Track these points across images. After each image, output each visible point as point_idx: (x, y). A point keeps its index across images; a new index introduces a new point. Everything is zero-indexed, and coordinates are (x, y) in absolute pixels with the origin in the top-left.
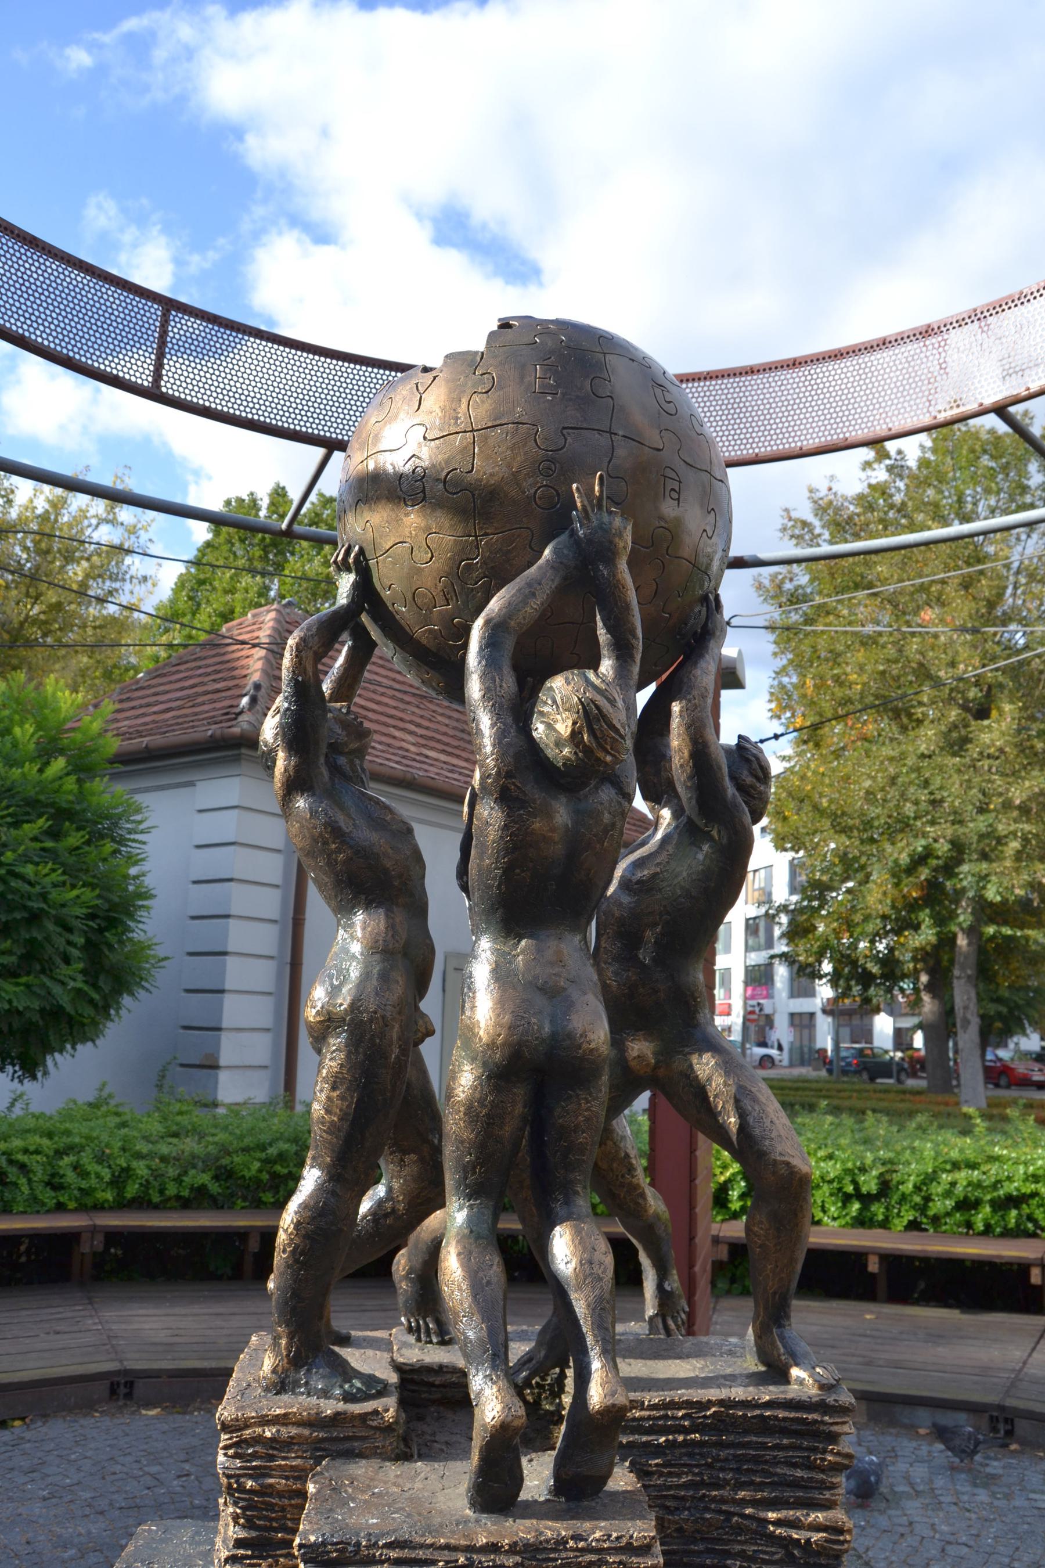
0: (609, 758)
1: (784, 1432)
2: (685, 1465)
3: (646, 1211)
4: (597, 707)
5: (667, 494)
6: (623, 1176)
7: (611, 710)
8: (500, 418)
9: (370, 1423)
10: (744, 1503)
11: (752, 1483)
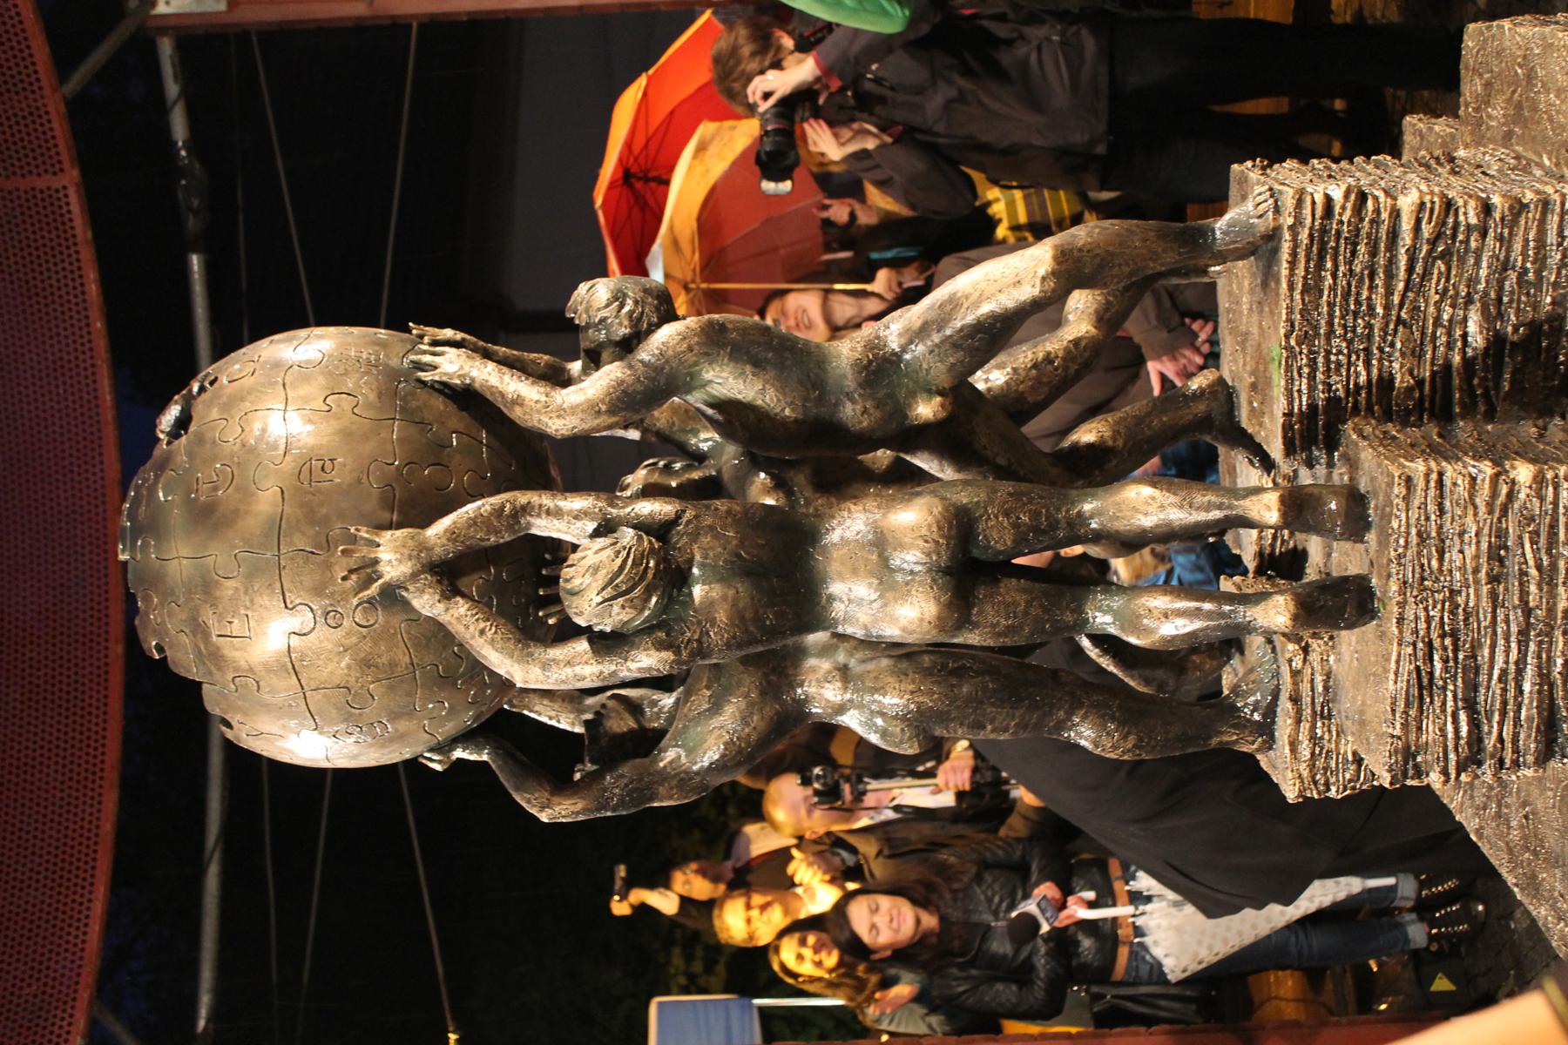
0: (652, 564)
1: (1320, 266)
2: (1348, 370)
4: (603, 589)
5: (329, 477)
6: (1056, 369)
7: (604, 571)
8: (287, 670)
9: (1299, 667)
10: (1387, 307)
11: (1369, 299)
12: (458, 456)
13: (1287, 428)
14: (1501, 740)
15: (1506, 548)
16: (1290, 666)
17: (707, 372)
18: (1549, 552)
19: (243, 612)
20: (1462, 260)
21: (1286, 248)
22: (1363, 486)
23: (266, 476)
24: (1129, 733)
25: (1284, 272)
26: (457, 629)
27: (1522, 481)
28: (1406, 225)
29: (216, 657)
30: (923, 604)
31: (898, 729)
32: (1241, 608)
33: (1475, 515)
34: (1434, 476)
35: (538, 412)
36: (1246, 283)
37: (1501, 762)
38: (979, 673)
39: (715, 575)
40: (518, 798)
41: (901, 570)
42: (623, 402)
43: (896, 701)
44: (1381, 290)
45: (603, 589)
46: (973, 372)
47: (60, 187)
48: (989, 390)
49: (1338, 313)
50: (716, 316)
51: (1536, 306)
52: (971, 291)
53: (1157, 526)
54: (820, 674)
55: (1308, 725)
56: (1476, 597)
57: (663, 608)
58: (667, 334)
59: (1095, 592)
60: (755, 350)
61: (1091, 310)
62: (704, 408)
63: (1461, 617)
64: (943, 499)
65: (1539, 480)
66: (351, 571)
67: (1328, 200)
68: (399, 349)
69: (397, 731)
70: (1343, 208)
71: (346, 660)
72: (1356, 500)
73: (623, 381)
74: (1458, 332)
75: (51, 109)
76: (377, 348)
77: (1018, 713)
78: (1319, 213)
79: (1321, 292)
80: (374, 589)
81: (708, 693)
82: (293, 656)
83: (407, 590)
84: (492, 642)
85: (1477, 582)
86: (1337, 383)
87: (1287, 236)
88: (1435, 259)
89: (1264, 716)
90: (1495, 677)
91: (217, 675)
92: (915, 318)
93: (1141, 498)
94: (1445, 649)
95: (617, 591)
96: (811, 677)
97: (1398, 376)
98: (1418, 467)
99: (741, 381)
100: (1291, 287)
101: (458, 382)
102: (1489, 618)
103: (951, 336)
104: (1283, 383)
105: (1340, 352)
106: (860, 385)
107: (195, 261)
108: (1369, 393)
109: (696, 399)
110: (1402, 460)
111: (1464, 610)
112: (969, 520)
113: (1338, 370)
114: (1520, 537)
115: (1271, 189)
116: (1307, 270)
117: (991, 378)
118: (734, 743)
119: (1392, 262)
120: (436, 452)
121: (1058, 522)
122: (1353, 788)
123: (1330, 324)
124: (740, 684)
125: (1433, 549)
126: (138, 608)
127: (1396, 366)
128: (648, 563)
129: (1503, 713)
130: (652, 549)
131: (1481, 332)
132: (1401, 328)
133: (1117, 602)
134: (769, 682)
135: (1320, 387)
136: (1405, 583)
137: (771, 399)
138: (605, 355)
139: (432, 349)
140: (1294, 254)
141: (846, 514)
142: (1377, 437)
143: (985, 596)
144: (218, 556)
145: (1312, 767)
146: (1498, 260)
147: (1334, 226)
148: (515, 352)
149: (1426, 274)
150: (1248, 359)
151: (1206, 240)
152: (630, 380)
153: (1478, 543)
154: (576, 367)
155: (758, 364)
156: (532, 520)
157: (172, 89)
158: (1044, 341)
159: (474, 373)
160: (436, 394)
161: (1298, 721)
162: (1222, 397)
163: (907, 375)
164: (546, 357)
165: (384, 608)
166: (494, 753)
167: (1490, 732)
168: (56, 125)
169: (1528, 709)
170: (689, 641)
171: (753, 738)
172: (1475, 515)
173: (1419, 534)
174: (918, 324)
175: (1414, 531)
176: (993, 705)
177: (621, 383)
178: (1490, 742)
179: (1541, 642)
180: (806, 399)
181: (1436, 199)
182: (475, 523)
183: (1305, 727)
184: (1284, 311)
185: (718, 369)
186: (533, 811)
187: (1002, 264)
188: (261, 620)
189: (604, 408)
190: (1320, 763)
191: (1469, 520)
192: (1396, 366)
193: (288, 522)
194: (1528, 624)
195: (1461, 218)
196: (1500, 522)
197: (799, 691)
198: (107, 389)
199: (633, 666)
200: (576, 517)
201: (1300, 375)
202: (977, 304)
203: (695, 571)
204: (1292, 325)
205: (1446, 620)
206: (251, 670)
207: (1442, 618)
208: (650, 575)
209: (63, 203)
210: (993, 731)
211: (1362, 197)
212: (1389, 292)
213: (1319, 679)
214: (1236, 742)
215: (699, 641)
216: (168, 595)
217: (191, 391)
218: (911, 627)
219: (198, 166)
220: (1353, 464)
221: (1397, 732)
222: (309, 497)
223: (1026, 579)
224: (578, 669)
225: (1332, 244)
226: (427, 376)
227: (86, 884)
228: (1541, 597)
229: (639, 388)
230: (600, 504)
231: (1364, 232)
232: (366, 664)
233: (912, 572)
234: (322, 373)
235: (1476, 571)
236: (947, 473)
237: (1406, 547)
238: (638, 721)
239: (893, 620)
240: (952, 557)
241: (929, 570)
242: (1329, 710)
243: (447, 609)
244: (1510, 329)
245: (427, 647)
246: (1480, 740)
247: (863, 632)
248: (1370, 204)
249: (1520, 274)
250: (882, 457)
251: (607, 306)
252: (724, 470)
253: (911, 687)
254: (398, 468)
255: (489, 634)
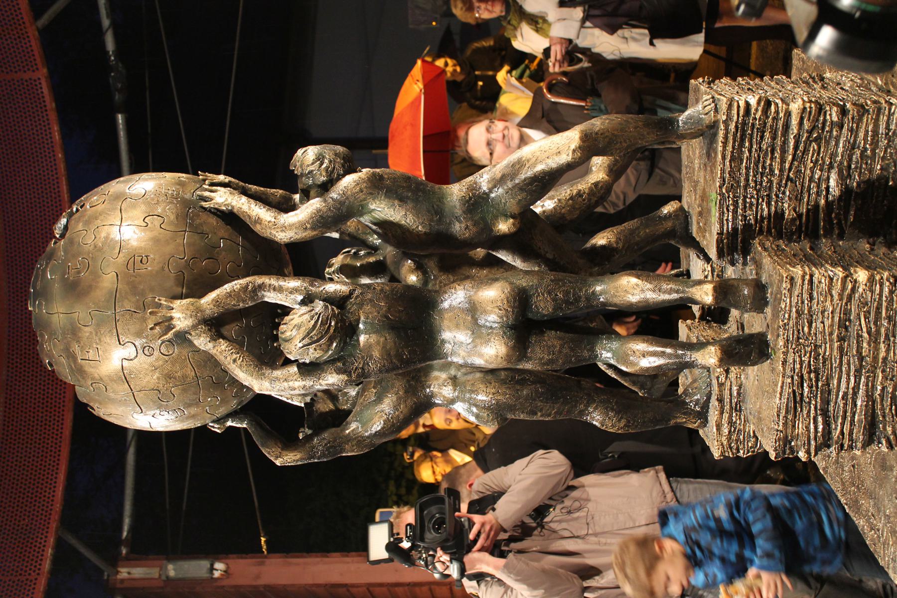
0: (333, 324)
1: (742, 145)
2: (757, 208)
3: (606, 181)
4: (303, 339)
6: (584, 200)
10: (781, 170)
11: (771, 165)
12: (224, 253)
13: (719, 242)
14: (842, 433)
15: (850, 321)
16: (718, 381)
17: (372, 204)
18: (875, 324)
19: (95, 346)
20: (828, 143)
21: (721, 134)
22: (764, 279)
23: (108, 266)
24: (622, 418)
25: (720, 149)
26: (221, 358)
27: (861, 281)
28: (794, 121)
29: (80, 371)
30: (497, 347)
31: (486, 415)
32: (689, 353)
33: (832, 301)
34: (807, 277)
35: (270, 228)
36: (697, 152)
37: (842, 446)
38: (533, 383)
39: (372, 329)
40: (264, 451)
41: (484, 326)
42: (320, 223)
43: (484, 398)
44: (778, 160)
45: (303, 339)
46: (533, 203)
47: (36, 78)
48: (544, 212)
49: (751, 174)
50: (378, 170)
51: (871, 171)
52: (531, 157)
53: (639, 302)
54: (441, 381)
55: (727, 415)
56: (830, 350)
57: (342, 348)
58: (349, 180)
59: (602, 339)
60: (400, 191)
61: (606, 165)
62: (370, 225)
63: (821, 361)
64: (511, 283)
65: (871, 280)
66: (156, 325)
67: (748, 104)
68: (192, 187)
69: (190, 413)
70: (757, 110)
71: (157, 375)
72: (759, 288)
73: (320, 210)
74: (824, 186)
75: (30, 34)
76: (178, 187)
77: (557, 406)
78: (741, 113)
79: (742, 160)
80: (170, 335)
81: (375, 391)
82: (125, 372)
83: (191, 334)
84: (240, 366)
85: (831, 340)
86: (749, 215)
87: (722, 127)
88: (811, 142)
89: (702, 408)
90: (840, 396)
91: (82, 382)
92: (497, 172)
93: (630, 285)
94: (811, 380)
95: (311, 339)
96: (435, 382)
97: (787, 212)
98: (798, 271)
99: (392, 210)
100: (724, 158)
101: (224, 208)
102: (838, 361)
103: (518, 184)
104: (717, 214)
105: (752, 197)
106: (464, 212)
107: (120, 118)
108: (769, 221)
109: (366, 219)
110: (788, 266)
111: (823, 357)
112: (527, 296)
113: (751, 208)
114: (859, 315)
115: (713, 97)
116: (733, 148)
117: (545, 205)
118: (389, 421)
119: (785, 143)
120: (211, 251)
121: (580, 297)
122: (753, 452)
123: (747, 180)
124: (393, 386)
125: (806, 320)
126: (38, 341)
127: (786, 205)
128: (331, 323)
129: (844, 418)
130: (334, 315)
131: (838, 186)
132: (789, 183)
133: (615, 345)
134: (410, 385)
135: (740, 218)
136: (788, 340)
137: (411, 220)
138: (312, 193)
139: (210, 188)
140: (726, 137)
141: (453, 291)
142: (772, 248)
143: (536, 341)
144: (81, 313)
145: (729, 439)
146: (849, 143)
147: (751, 121)
148: (262, 189)
149: (806, 151)
150: (697, 197)
151: (673, 128)
152: (325, 209)
153: (833, 317)
154: (297, 197)
155: (402, 200)
156: (265, 293)
157: (106, 22)
158: (578, 182)
159: (234, 203)
160: (211, 216)
161: (722, 413)
162: (682, 218)
163: (493, 206)
164: (281, 191)
165: (178, 344)
166: (253, 421)
167: (836, 429)
168: (33, 43)
169: (859, 416)
170: (356, 368)
171: (401, 417)
172: (832, 301)
173: (797, 312)
174: (499, 175)
175: (794, 310)
176: (541, 401)
177: (319, 211)
178: (836, 434)
179: (868, 377)
180: (431, 220)
181: (813, 105)
182: (230, 296)
183: (726, 416)
184: (719, 172)
185: (378, 203)
186: (272, 459)
187: (549, 141)
188: (105, 351)
189: (309, 226)
190: (734, 437)
191: (828, 303)
192: (786, 205)
193: (120, 293)
194: (861, 366)
195: (828, 117)
196: (847, 305)
197: (428, 390)
198: (65, 191)
199: (323, 383)
200: (291, 293)
201: (728, 210)
202: (534, 165)
203: (361, 326)
204: (724, 180)
205: (812, 363)
206: (101, 379)
207: (809, 362)
208: (332, 330)
209: (38, 88)
210: (541, 416)
211: (768, 103)
212: (783, 161)
213: (735, 388)
214: (685, 422)
215: (363, 368)
216: (52, 334)
217: (72, 210)
218: (492, 360)
219: (120, 65)
220: (758, 265)
221: (781, 428)
222: (133, 278)
223: (560, 331)
224: (291, 384)
225: (749, 132)
226: (206, 205)
227: (55, 464)
228: (870, 351)
229: (330, 214)
230: (305, 285)
231: (768, 125)
232: (168, 377)
233: (491, 327)
234: (144, 203)
235: (831, 334)
236: (518, 263)
237: (789, 319)
238: (334, 405)
239: (481, 355)
240: (516, 319)
241: (502, 327)
242: (740, 407)
243: (214, 347)
244: (855, 184)
245: (205, 366)
246: (830, 433)
247: (463, 361)
248: (773, 107)
249: (862, 151)
250: (480, 252)
251: (313, 164)
252: (388, 257)
253: (493, 390)
254: (186, 261)
255: (239, 362)
